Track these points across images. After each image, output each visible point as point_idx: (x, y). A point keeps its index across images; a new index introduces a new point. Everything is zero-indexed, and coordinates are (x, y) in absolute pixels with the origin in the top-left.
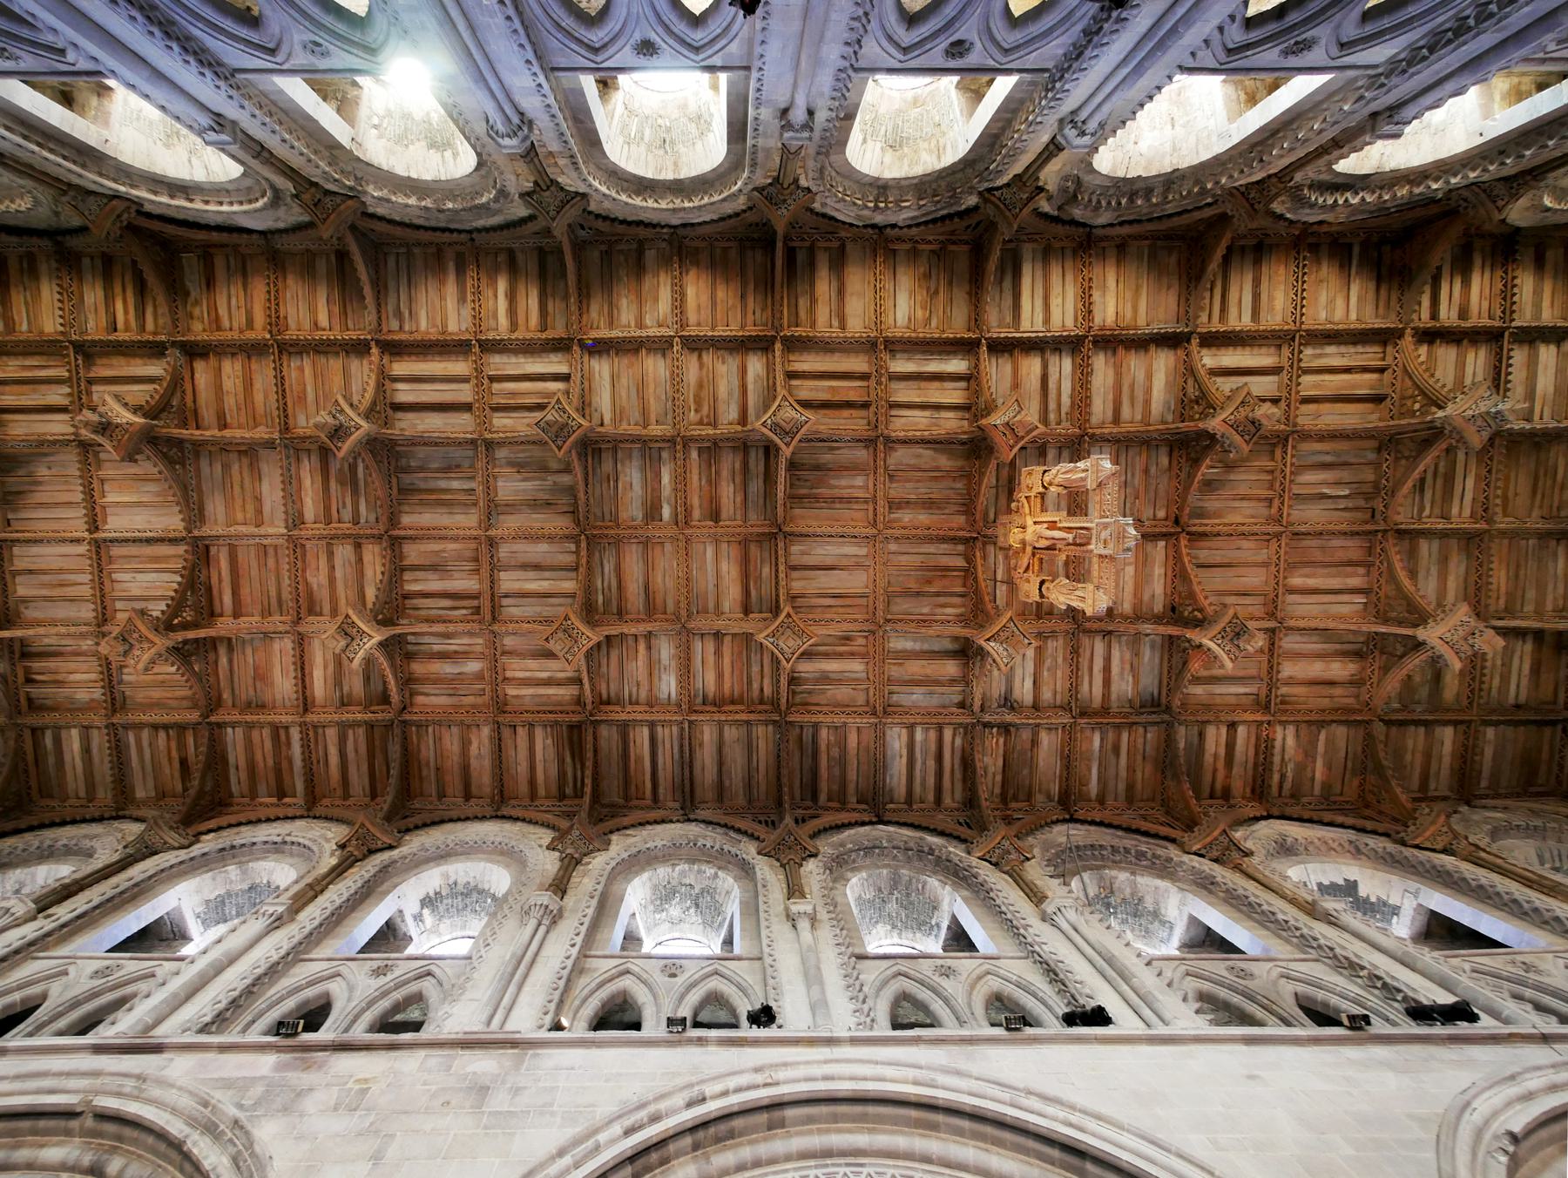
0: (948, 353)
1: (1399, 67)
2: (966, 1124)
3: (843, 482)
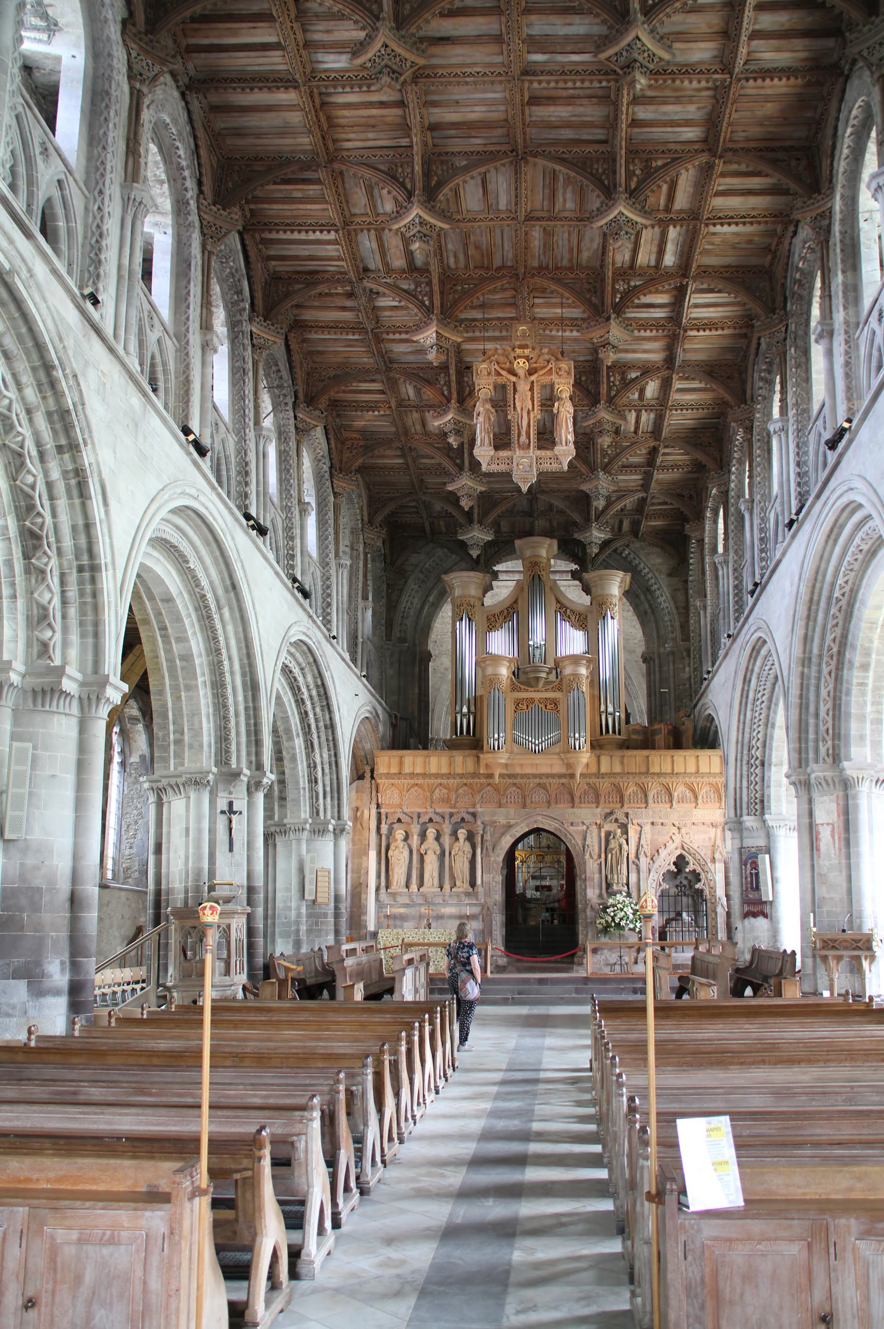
0: (681, 256)
2: (218, 553)
3: (569, 195)
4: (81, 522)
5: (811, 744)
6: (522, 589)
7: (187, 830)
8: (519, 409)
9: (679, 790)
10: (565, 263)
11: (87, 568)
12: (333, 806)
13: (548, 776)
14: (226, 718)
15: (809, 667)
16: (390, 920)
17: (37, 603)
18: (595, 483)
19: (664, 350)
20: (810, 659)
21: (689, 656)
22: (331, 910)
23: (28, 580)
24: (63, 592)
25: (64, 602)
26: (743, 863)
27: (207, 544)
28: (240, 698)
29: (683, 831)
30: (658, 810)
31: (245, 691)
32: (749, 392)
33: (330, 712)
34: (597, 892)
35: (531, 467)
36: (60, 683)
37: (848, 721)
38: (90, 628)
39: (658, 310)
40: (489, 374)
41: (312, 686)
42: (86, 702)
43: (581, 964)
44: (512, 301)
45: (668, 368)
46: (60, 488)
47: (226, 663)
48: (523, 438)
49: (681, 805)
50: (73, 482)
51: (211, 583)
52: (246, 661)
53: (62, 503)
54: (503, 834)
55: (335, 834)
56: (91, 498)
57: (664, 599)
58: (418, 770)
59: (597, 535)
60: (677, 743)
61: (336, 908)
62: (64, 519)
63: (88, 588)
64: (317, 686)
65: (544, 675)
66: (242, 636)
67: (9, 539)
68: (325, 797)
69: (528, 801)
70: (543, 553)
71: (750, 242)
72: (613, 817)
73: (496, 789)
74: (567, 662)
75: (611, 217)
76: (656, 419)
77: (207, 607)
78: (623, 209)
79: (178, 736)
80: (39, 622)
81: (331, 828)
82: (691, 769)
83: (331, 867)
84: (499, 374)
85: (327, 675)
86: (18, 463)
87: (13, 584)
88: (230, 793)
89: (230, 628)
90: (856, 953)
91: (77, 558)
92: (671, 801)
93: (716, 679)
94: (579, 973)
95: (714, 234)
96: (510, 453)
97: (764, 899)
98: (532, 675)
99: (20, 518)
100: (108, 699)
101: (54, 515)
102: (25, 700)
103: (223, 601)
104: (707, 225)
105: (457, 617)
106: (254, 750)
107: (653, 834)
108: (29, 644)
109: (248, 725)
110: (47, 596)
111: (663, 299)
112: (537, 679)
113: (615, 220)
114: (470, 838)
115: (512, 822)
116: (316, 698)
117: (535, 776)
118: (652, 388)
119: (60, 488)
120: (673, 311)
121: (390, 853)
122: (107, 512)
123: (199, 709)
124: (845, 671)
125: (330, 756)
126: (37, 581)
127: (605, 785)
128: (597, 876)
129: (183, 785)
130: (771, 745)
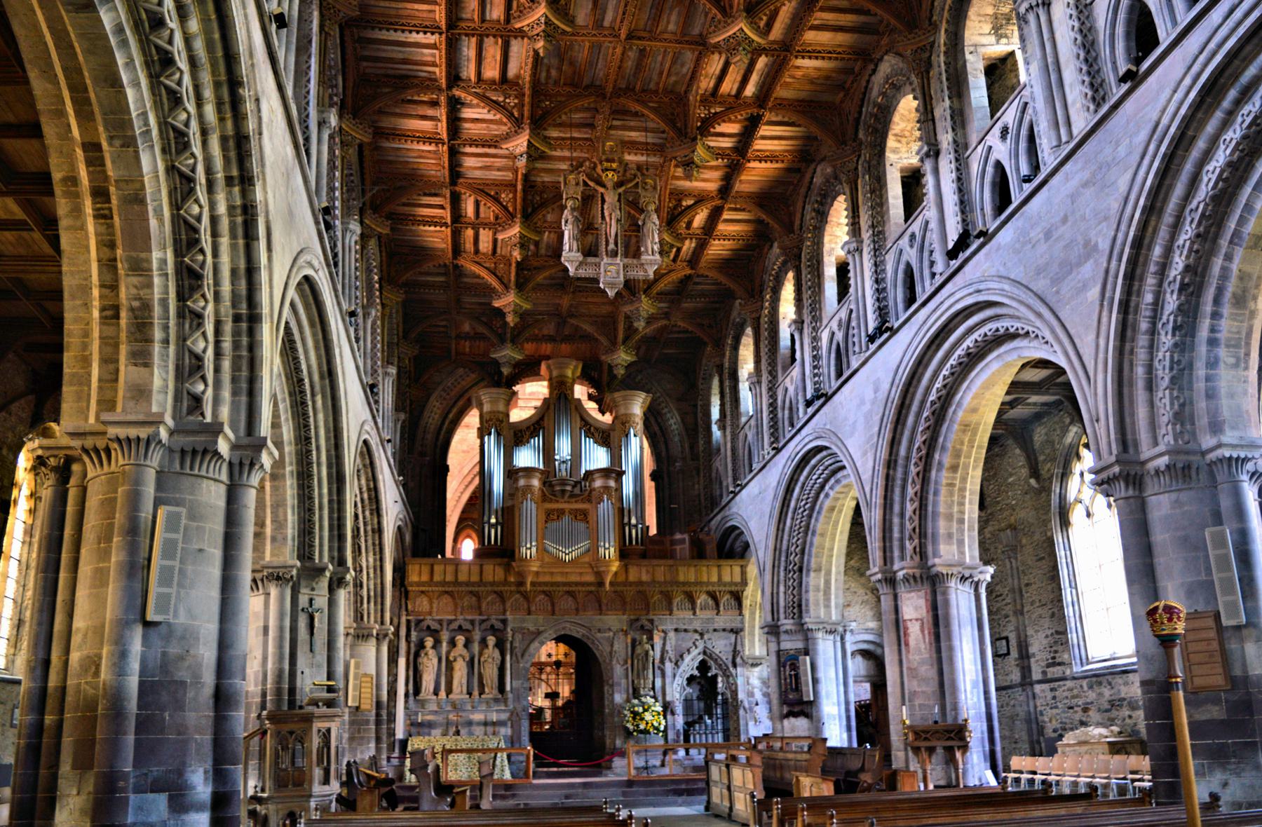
1: (815, 339)
3: (674, 18)
4: (242, 265)
5: (896, 544)
6: (548, 408)
7: (266, 629)
8: (608, 219)
9: (702, 599)
10: (652, 86)
11: (244, 318)
12: (376, 611)
13: (577, 584)
14: (311, 510)
15: (895, 469)
16: (416, 727)
17: (191, 352)
18: (636, 305)
19: (722, 180)
20: (896, 461)
21: (698, 474)
22: (373, 718)
23: (180, 325)
24: (218, 343)
25: (218, 354)
26: (781, 664)
27: (312, 325)
28: (325, 491)
29: (706, 637)
30: (682, 616)
31: (329, 483)
32: (797, 223)
33: (379, 516)
34: (625, 696)
35: (618, 273)
36: (216, 443)
37: (934, 520)
38: (244, 386)
39: (726, 139)
40: (577, 184)
41: (365, 489)
42: (236, 469)
43: (609, 768)
44: (589, 121)
45: (722, 198)
46: (224, 224)
47: (314, 453)
48: (611, 246)
49: (704, 612)
50: (239, 219)
51: (309, 367)
52: (333, 452)
53: (225, 241)
54: (532, 641)
55: (377, 639)
56: (258, 239)
57: (674, 422)
58: (449, 578)
59: (623, 357)
60: (699, 552)
61: (378, 715)
62: (225, 259)
63: (245, 340)
64: (369, 490)
65: (569, 488)
66: (331, 425)
67: (167, 275)
68: (369, 602)
69: (557, 609)
70: (569, 373)
71: (827, 78)
72: (639, 624)
73: (525, 595)
74: (597, 475)
75: (731, 33)
76: (696, 248)
77: (302, 392)
78: (741, 26)
79: (258, 529)
80: (191, 374)
81: (375, 632)
82: (715, 579)
83: (374, 673)
84: (585, 184)
85: (380, 477)
86: (186, 189)
87: (166, 328)
88: (313, 589)
89: (321, 416)
90: (949, 743)
91: (234, 306)
92: (694, 609)
93: (744, 492)
94: (610, 777)
95: (798, 67)
96: (597, 260)
97: (805, 699)
98: (558, 488)
99: (178, 254)
100: (262, 466)
101: (215, 254)
102: (171, 461)
103: (318, 388)
104: (796, 57)
105: (482, 433)
106: (336, 545)
107: (677, 640)
108: (177, 398)
109: (331, 518)
110: (202, 344)
111: (733, 128)
112: (563, 492)
113: (733, 36)
114: (500, 645)
115: (541, 629)
116: (367, 502)
117: (565, 584)
118: (700, 219)
119: (224, 224)
120: (739, 142)
121: (420, 660)
122: (270, 259)
123: (285, 500)
124: (933, 473)
125: (375, 560)
126: (191, 327)
127: (630, 592)
128: (624, 681)
129: (262, 580)
130: (810, 551)
